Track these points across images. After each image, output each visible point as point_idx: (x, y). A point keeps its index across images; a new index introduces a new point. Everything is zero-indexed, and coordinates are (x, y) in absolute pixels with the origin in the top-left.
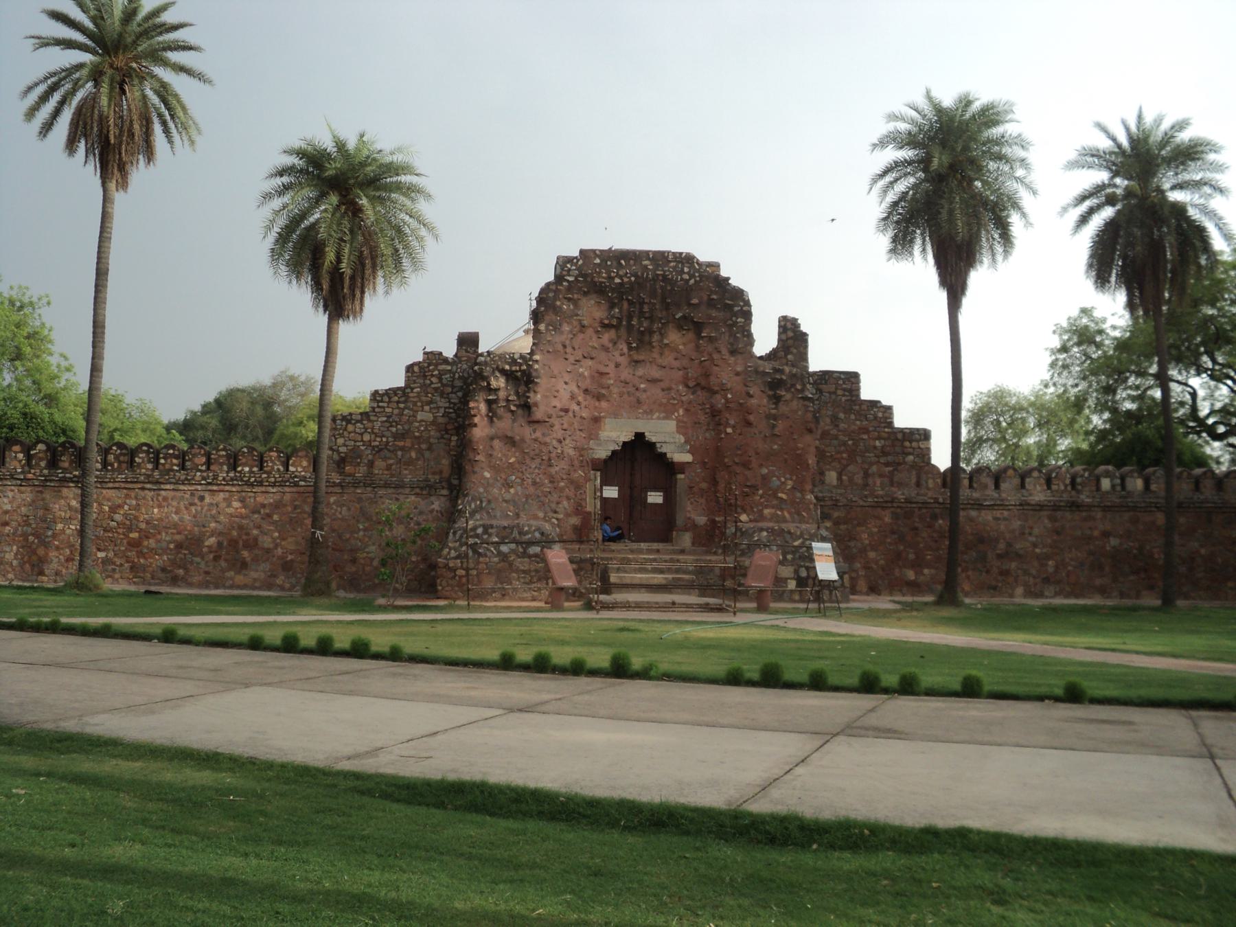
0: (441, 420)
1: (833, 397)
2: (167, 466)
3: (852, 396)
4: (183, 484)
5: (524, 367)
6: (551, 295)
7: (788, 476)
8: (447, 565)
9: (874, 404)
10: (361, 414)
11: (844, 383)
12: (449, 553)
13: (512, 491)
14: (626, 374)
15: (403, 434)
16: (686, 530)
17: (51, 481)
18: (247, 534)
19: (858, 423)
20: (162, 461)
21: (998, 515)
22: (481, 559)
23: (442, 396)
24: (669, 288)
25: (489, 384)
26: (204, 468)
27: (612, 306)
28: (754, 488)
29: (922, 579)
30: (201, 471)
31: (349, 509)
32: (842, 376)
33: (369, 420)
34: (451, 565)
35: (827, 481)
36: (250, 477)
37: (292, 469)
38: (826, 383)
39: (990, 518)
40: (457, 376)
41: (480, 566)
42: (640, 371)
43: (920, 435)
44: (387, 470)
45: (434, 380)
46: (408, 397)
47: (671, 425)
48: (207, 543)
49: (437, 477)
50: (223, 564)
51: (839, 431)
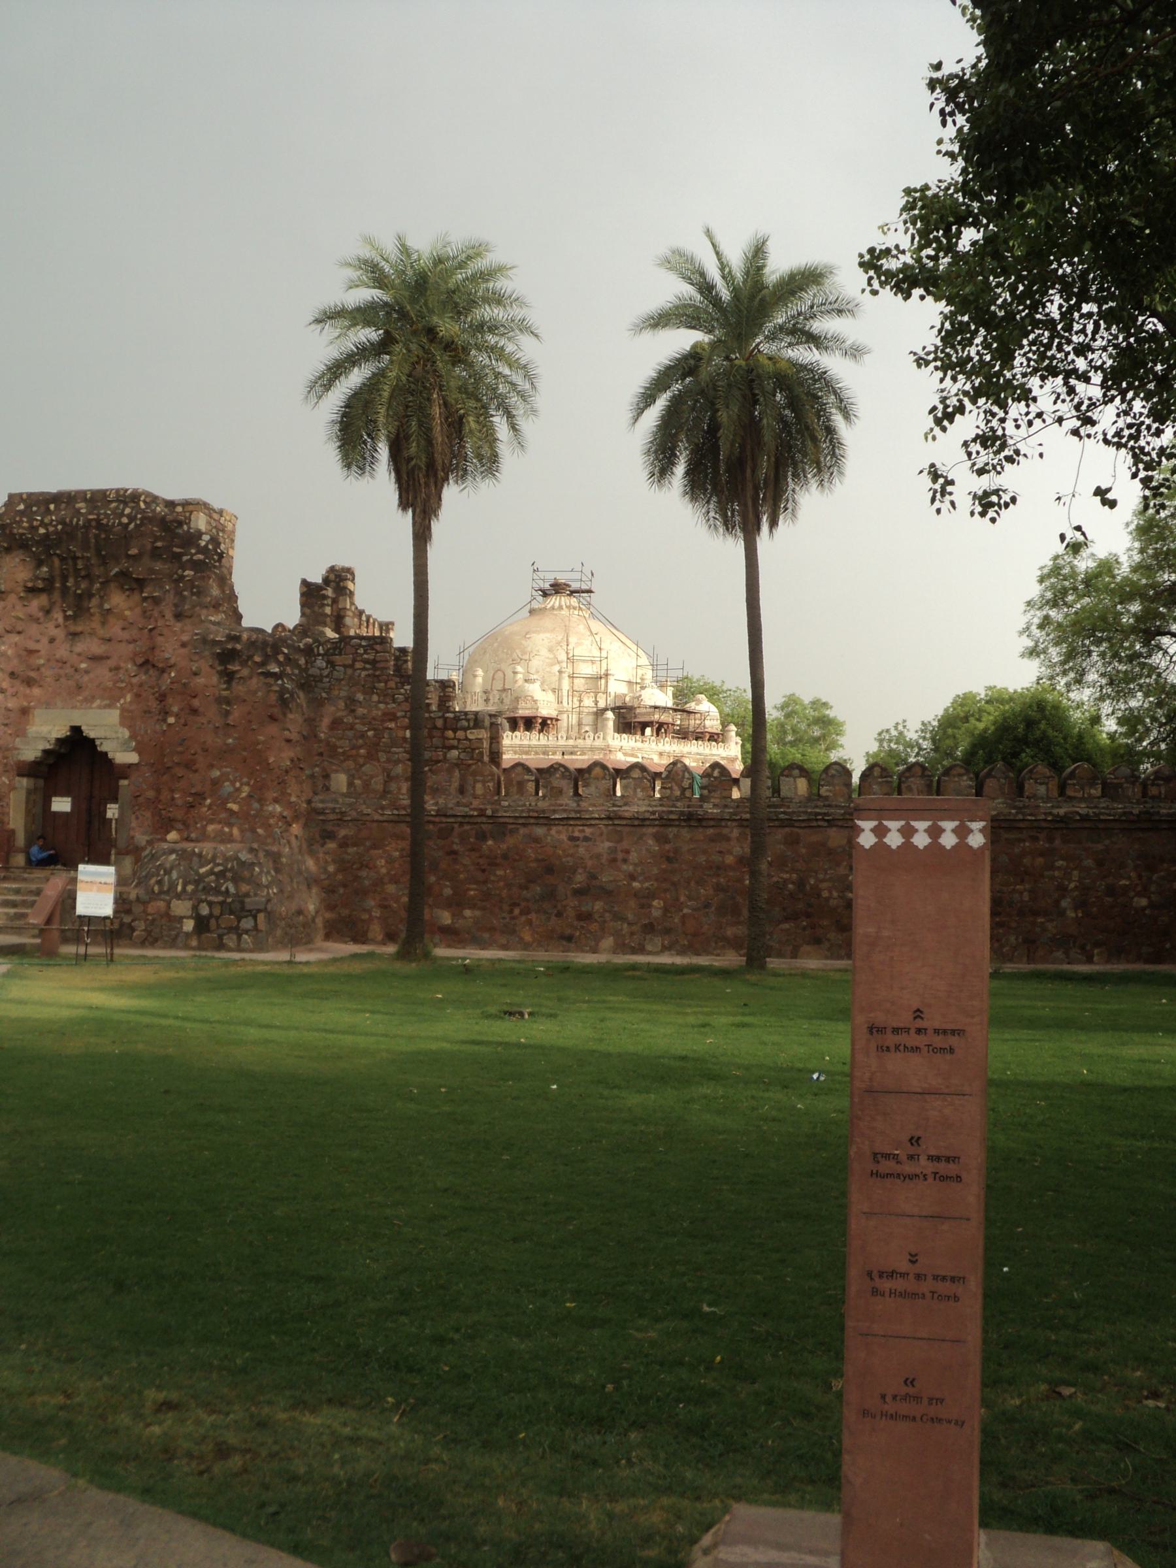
1: (349, 671)
3: (375, 669)
7: (245, 780)
11: (366, 652)
19: (382, 706)
21: (576, 834)
24: (103, 536)
27: (40, 564)
28: (201, 796)
29: (460, 923)
32: (364, 643)
35: (333, 785)
38: (340, 654)
39: (564, 837)
42: (80, 647)
43: (468, 720)
47: (113, 716)
51: (356, 718)
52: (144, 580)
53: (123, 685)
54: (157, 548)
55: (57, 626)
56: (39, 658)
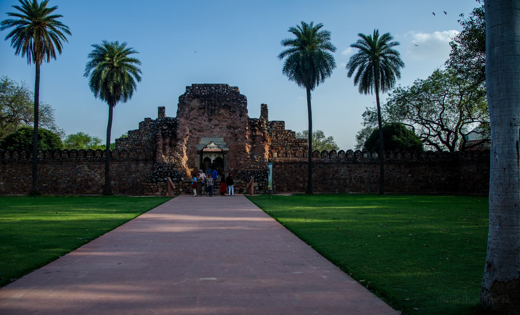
0: (150, 140)
2: (64, 157)
4: (69, 162)
5: (174, 122)
6: (182, 99)
7: (259, 155)
9: (289, 131)
10: (125, 138)
12: (148, 181)
16: (227, 172)
17: (27, 162)
18: (90, 177)
20: (63, 155)
22: (158, 183)
23: (151, 132)
25: (162, 128)
26: (76, 157)
27: (202, 102)
30: (75, 158)
31: (122, 168)
33: (128, 140)
35: (274, 156)
36: (90, 159)
40: (155, 126)
45: (148, 127)
46: (140, 132)
48: (77, 180)
50: (83, 187)
55: (206, 117)
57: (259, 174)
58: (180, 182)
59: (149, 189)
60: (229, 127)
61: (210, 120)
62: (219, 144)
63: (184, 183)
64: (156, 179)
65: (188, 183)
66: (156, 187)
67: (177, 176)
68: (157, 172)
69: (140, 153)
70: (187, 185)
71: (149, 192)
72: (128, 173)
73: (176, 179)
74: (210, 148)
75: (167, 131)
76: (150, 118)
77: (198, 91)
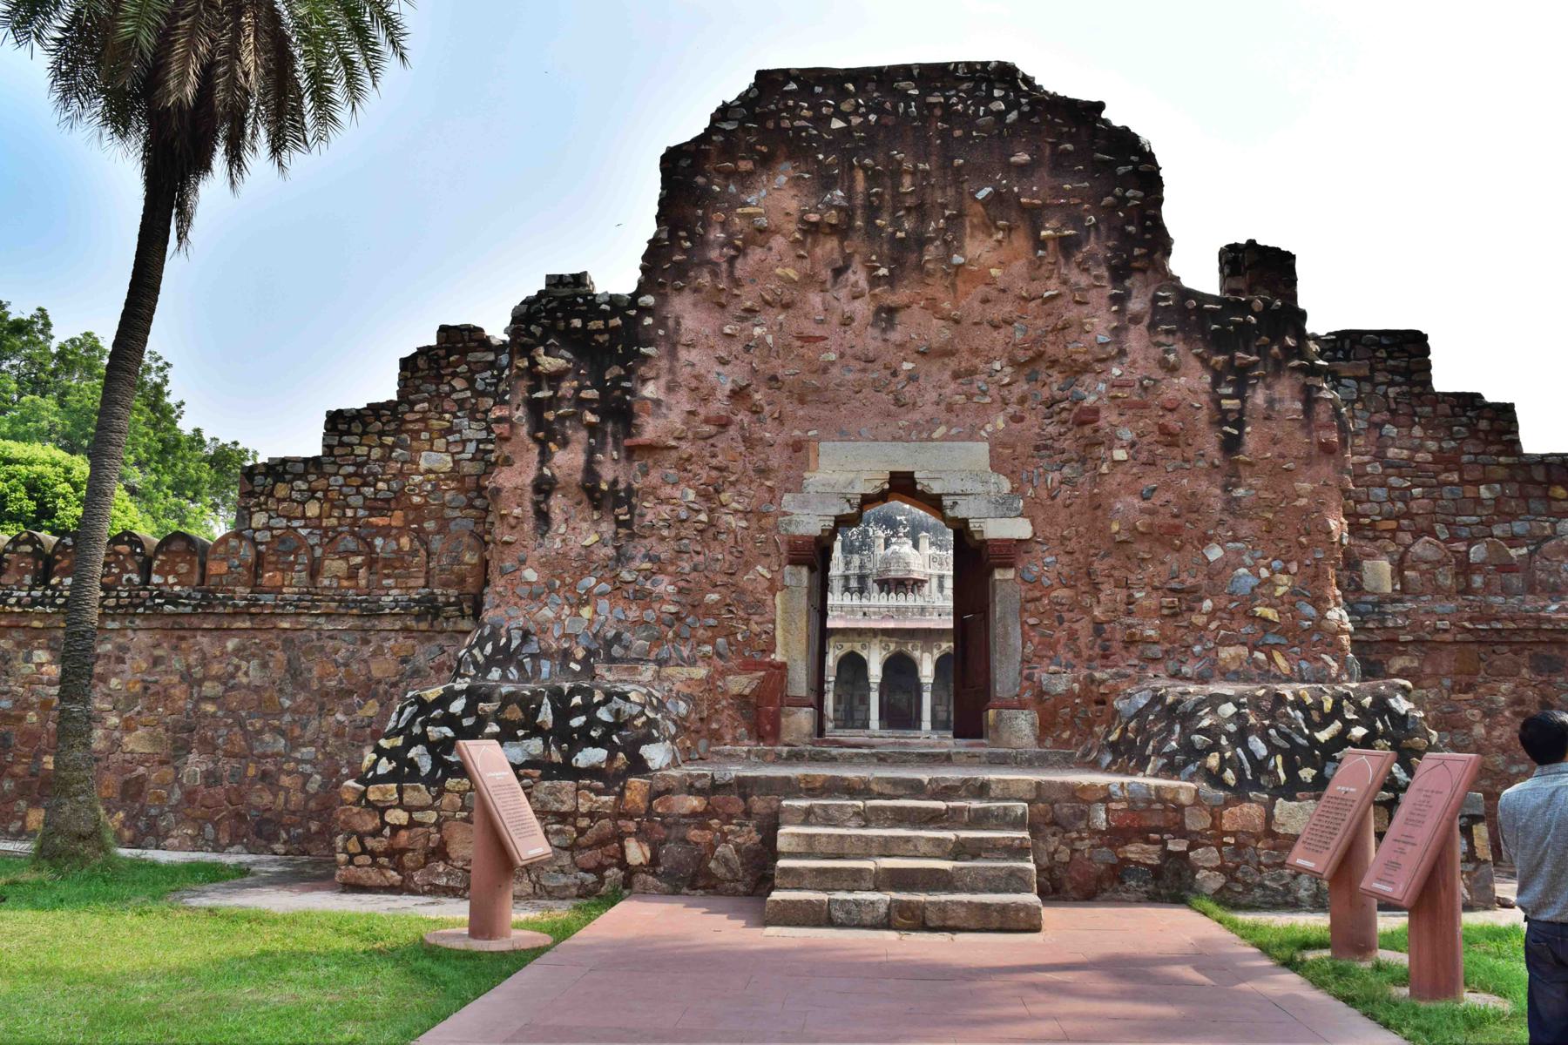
0: (468, 468)
1: (1367, 388)
3: (1412, 384)
5: (617, 321)
7: (1277, 564)
8: (364, 794)
9: (1470, 401)
13: (586, 612)
14: (871, 340)
15: (387, 501)
16: (1022, 706)
22: (451, 783)
23: (472, 418)
24: (958, 133)
25: (534, 363)
27: (826, 182)
28: (1190, 596)
31: (264, 665)
32: (1385, 341)
33: (323, 475)
34: (374, 794)
35: (1369, 583)
37: (156, 579)
38: (1346, 358)
41: (446, 799)
42: (896, 336)
44: (349, 578)
45: (458, 384)
46: (405, 422)
49: (452, 592)
52: (1044, 206)
53: (988, 400)
54: (1066, 153)
56: (827, 350)
57: (1326, 721)
58: (635, 781)
59: (376, 833)
60: (1030, 364)
61: (887, 315)
62: (957, 486)
63: (668, 791)
64: (439, 749)
65: (699, 792)
66: (431, 816)
67: (610, 728)
68: (450, 696)
69: (388, 563)
70: (694, 814)
71: (374, 864)
72: (300, 698)
73: (591, 756)
74: (865, 614)
75: (567, 387)
76: (481, 330)
77: (796, 105)
